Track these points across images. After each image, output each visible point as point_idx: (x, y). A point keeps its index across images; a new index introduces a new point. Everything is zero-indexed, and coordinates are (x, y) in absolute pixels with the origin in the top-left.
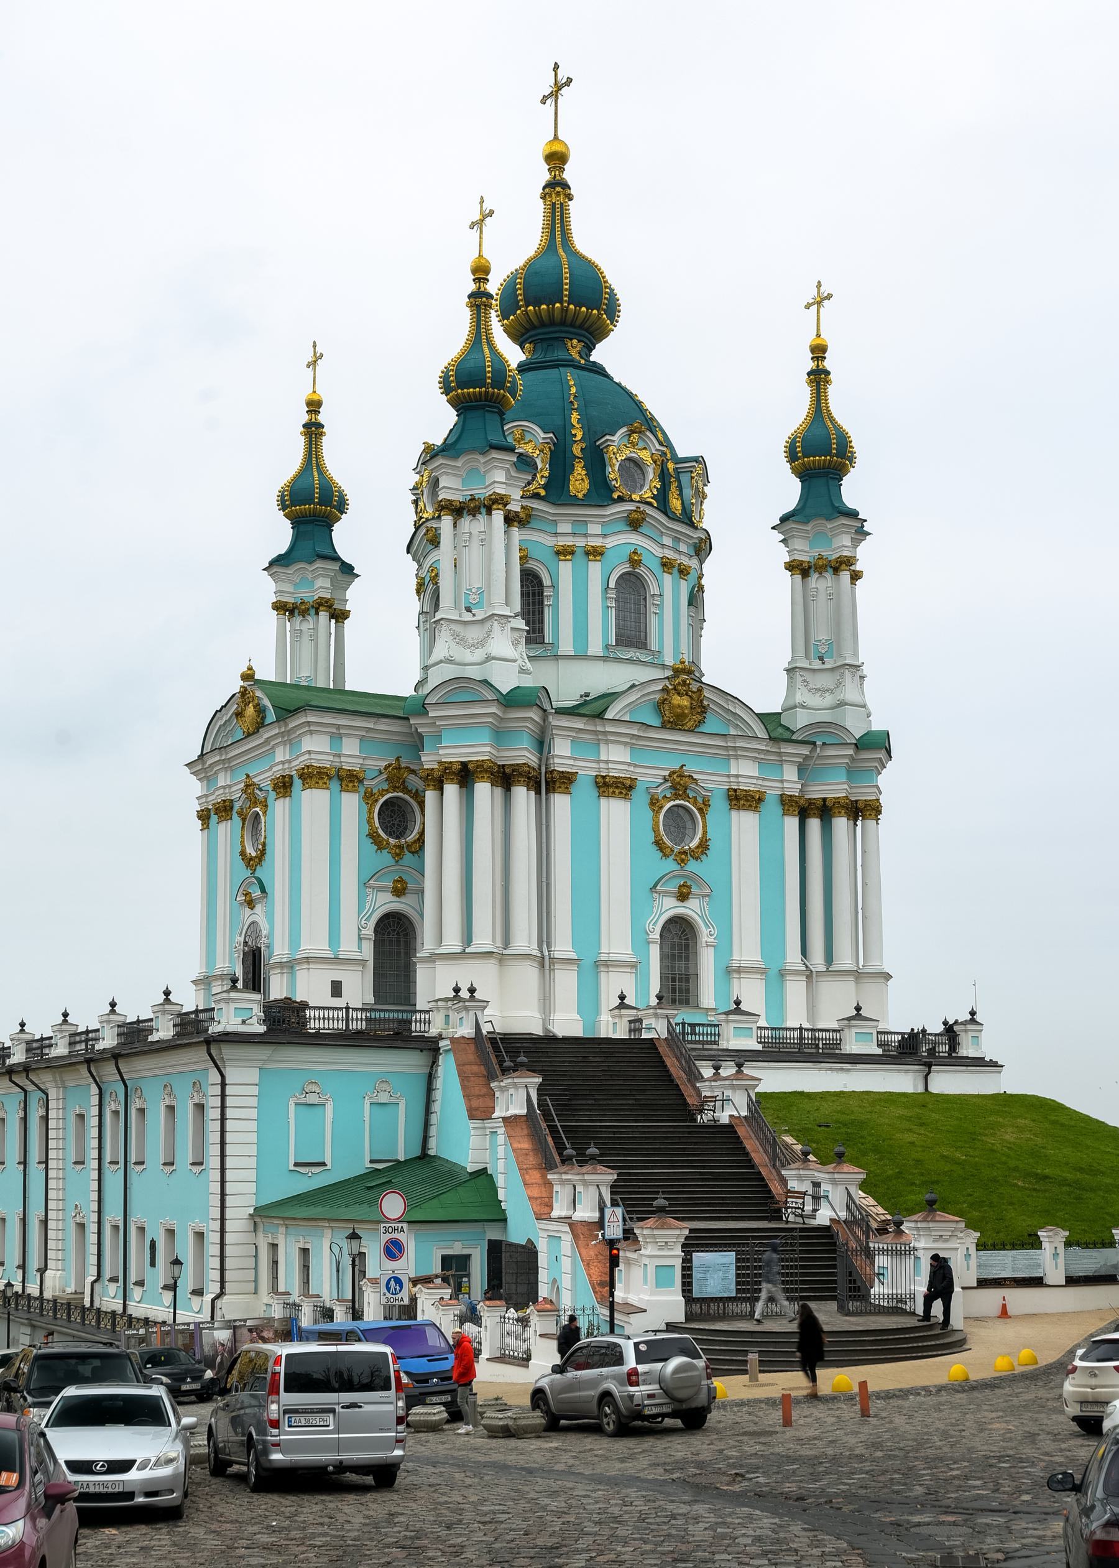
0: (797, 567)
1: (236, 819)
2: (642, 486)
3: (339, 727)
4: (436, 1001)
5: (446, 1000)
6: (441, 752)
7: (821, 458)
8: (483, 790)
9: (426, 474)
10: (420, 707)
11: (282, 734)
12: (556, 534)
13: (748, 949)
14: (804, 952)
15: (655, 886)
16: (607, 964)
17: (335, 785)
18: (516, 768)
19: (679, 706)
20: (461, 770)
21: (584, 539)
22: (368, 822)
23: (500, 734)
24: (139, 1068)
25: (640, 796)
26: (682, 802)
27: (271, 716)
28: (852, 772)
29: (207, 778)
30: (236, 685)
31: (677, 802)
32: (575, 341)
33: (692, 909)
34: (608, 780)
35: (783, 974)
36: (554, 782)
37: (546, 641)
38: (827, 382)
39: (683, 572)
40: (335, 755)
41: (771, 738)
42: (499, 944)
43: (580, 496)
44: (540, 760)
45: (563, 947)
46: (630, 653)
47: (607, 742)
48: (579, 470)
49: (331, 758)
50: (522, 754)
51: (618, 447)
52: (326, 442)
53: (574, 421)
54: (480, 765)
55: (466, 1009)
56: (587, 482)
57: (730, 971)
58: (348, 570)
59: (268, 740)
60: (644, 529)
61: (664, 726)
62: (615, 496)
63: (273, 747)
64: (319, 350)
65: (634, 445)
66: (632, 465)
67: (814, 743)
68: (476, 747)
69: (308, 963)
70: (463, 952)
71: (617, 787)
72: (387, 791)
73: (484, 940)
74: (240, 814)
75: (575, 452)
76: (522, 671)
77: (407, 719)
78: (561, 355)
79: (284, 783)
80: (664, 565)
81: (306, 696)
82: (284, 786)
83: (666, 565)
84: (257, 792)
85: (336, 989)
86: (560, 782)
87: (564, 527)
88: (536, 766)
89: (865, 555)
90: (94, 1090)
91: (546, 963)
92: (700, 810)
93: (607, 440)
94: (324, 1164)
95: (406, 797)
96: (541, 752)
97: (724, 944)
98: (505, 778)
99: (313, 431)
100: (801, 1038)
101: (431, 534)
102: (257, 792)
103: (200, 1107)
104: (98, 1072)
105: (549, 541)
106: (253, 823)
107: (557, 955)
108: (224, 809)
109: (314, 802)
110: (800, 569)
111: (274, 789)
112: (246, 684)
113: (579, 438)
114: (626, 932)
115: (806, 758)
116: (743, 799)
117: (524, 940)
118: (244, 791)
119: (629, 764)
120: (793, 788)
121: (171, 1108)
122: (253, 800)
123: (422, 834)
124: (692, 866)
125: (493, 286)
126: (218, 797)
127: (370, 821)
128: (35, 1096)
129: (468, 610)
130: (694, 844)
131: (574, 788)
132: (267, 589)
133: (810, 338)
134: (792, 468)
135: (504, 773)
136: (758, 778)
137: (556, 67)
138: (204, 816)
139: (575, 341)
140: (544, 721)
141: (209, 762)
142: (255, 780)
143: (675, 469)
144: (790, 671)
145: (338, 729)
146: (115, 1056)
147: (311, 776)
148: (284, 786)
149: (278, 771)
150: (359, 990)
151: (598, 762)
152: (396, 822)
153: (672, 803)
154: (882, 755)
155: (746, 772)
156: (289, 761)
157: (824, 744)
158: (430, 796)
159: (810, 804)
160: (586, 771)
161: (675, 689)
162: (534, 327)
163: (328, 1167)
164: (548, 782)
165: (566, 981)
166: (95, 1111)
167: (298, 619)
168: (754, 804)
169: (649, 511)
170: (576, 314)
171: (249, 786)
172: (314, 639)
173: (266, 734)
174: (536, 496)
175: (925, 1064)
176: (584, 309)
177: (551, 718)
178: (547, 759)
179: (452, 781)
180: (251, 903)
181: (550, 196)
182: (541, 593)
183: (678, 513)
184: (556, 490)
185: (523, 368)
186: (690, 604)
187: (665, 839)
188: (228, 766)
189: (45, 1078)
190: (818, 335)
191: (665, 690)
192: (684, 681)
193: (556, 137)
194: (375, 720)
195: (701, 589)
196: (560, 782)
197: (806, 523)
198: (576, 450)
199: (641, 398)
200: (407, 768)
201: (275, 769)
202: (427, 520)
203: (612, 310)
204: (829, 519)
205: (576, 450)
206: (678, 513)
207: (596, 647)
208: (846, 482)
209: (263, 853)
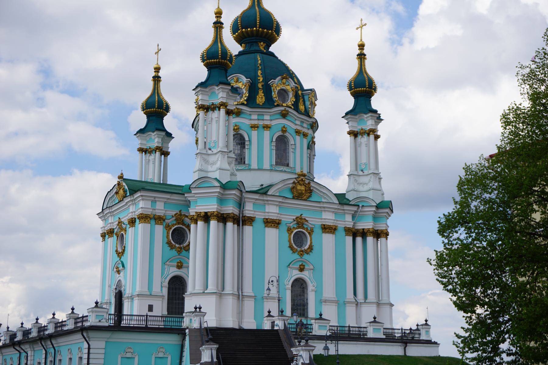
1: (115, 237)
2: (288, 100)
3: (155, 197)
6: (197, 208)
7: (363, 89)
8: (213, 223)
10: (189, 189)
12: (251, 119)
13: (329, 292)
14: (355, 294)
15: (289, 265)
17: (153, 222)
18: (228, 214)
19: (300, 190)
21: (262, 121)
22: (167, 237)
23: (221, 200)
24: (61, 342)
26: (301, 230)
27: (128, 194)
28: (375, 218)
29: (105, 220)
31: (299, 230)
33: (305, 275)
35: (345, 303)
36: (245, 221)
37: (246, 163)
38: (365, 59)
39: (305, 135)
40: (153, 209)
41: (340, 204)
42: (220, 288)
43: (261, 104)
44: (240, 211)
47: (269, 204)
48: (261, 93)
49: (151, 210)
50: (230, 208)
51: (277, 84)
53: (259, 74)
55: (196, 316)
56: (264, 98)
57: (321, 301)
60: (288, 118)
61: (294, 198)
62: (276, 104)
64: (160, 47)
65: (284, 84)
66: (283, 92)
67: (358, 206)
68: (211, 206)
70: (204, 293)
72: (176, 225)
73: (211, 288)
74: (116, 234)
76: (232, 174)
77: (184, 194)
78: (257, 48)
80: (296, 132)
81: (144, 185)
82: (132, 222)
83: (298, 132)
85: (151, 308)
86: (249, 221)
88: (238, 214)
89: (381, 129)
90: (44, 352)
91: (240, 296)
92: (309, 233)
95: (184, 227)
96: (240, 208)
97: (318, 291)
98: (223, 218)
100: (349, 331)
103: (81, 358)
105: (248, 122)
107: (245, 294)
108: (111, 232)
110: (354, 134)
113: (261, 81)
115: (356, 212)
116: (328, 229)
118: (118, 225)
120: (350, 225)
121: (71, 359)
122: (121, 229)
123: (189, 243)
124: (306, 256)
125: (228, 21)
126: (108, 228)
128: (24, 354)
130: (306, 247)
131: (254, 224)
134: (351, 93)
135: (223, 217)
136: (334, 220)
138: (103, 236)
139: (262, 43)
141: (105, 213)
142: (122, 220)
143: (302, 94)
146: (51, 337)
147: (142, 218)
148: (132, 222)
149: (130, 216)
150: (161, 308)
151: (265, 212)
152: (178, 237)
153: (297, 230)
154: (387, 210)
155: (329, 218)
156: (135, 212)
158: (192, 226)
160: (259, 216)
161: (298, 182)
162: (246, 38)
164: (242, 221)
165: (249, 305)
166: (43, 361)
167: (148, 155)
168: (333, 231)
169: (290, 110)
170: (263, 32)
174: (243, 104)
175: (404, 343)
177: (244, 194)
178: (243, 211)
180: (119, 272)
182: (244, 143)
183: (303, 111)
184: (251, 102)
185: (241, 54)
186: (308, 148)
187: (294, 245)
189: (26, 347)
190: (361, 40)
191: (294, 183)
192: (302, 179)
195: (314, 143)
196: (249, 221)
197: (356, 115)
198: (260, 86)
200: (184, 215)
203: (278, 30)
205: (260, 86)
206: (303, 111)
207: (267, 166)
208: (373, 99)
209: (124, 250)
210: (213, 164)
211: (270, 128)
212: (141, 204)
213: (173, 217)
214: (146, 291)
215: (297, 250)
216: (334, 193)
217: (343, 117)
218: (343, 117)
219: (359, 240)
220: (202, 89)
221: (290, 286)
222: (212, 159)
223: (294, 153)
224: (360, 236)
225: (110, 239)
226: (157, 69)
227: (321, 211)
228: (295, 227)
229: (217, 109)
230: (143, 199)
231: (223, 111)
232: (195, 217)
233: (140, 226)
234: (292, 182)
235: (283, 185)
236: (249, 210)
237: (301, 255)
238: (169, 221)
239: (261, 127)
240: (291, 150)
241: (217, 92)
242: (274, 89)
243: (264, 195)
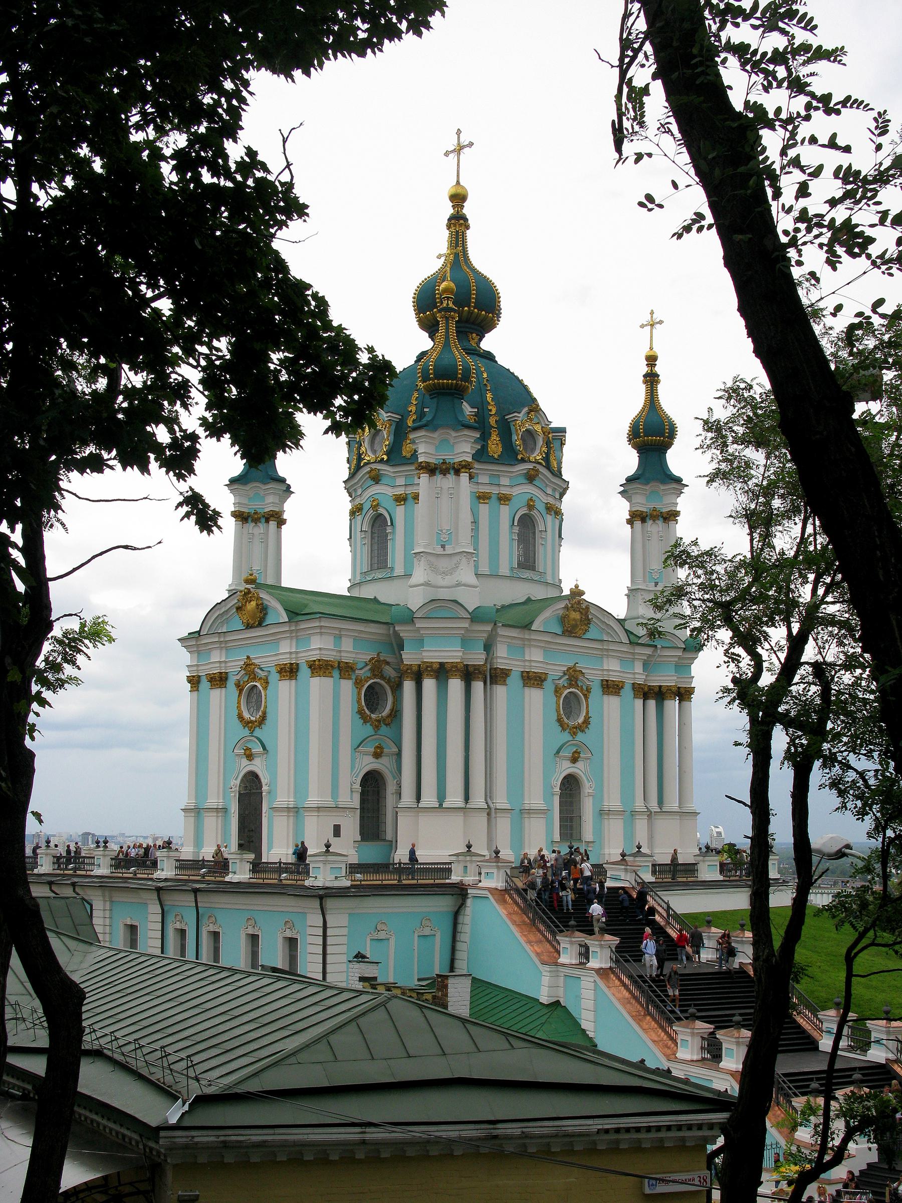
3: (341, 629)
8: (456, 685)
11: (291, 631)
16: (530, 811)
17: (336, 673)
19: (574, 619)
20: (440, 668)
23: (465, 642)
25: (549, 685)
29: (199, 652)
32: (474, 335)
33: (579, 769)
35: (633, 813)
36: (496, 676)
38: (658, 382)
43: (496, 456)
44: (486, 659)
45: (501, 801)
46: (527, 574)
47: (530, 646)
48: (495, 437)
53: (489, 400)
54: (454, 666)
56: (500, 446)
57: (603, 813)
62: (519, 457)
65: (531, 420)
69: (318, 811)
74: (238, 685)
84: (259, 671)
86: (497, 676)
91: (490, 812)
95: (382, 682)
98: (468, 674)
101: (373, 473)
109: (318, 687)
110: (635, 517)
113: (493, 412)
116: (611, 688)
120: (640, 679)
122: (253, 676)
124: (580, 736)
127: (359, 701)
130: (581, 720)
131: (509, 680)
133: (645, 351)
137: (459, 132)
138: (194, 682)
139: (474, 335)
147: (320, 667)
148: (290, 671)
149: (285, 660)
155: (613, 668)
158: (408, 686)
159: (650, 689)
161: (572, 607)
164: (497, 676)
165: (503, 825)
169: (542, 470)
170: (478, 315)
179: (431, 677)
181: (455, 225)
188: (224, 646)
190: (651, 349)
191: (566, 608)
193: (458, 182)
198: (492, 421)
204: (663, 482)
205: (492, 421)
207: (504, 570)
209: (264, 718)
213: (367, 665)
214: (328, 801)
219: (652, 703)
221: (557, 789)
224: (653, 698)
227: (602, 657)
229: (452, 472)
230: (321, 634)
236: (503, 656)
237: (575, 734)
238: (362, 672)
240: (539, 541)
241: (452, 441)
243: (527, 632)
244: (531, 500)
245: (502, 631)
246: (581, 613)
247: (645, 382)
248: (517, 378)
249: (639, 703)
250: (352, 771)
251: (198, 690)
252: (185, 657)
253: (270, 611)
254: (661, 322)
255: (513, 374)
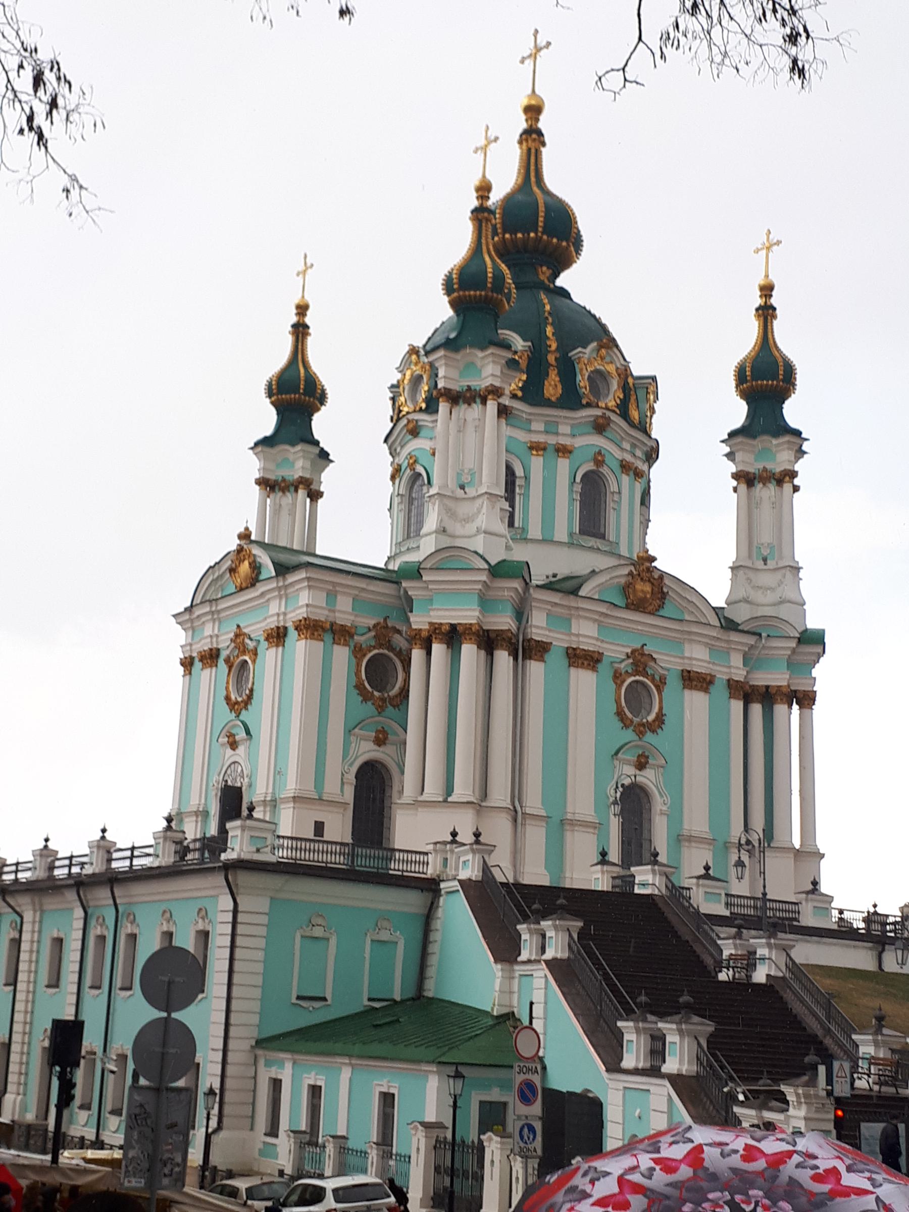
0: (740, 477)
2: (607, 395)
3: (334, 584)
4: (436, 843)
5: (445, 843)
6: (432, 613)
7: (766, 381)
8: (469, 651)
9: (408, 373)
12: (530, 431)
17: (328, 637)
18: (500, 633)
19: (642, 591)
20: (449, 632)
22: (356, 674)
26: (641, 678)
29: (193, 629)
30: (233, 544)
32: (544, 269)
34: (578, 652)
36: (531, 650)
37: (516, 525)
38: (774, 317)
40: (330, 610)
43: (553, 399)
44: (518, 629)
46: (592, 542)
48: (553, 377)
49: (326, 612)
52: (311, 343)
56: (560, 387)
58: (324, 456)
59: (263, 594)
61: (627, 607)
62: (584, 402)
63: (268, 600)
65: (602, 358)
68: (466, 614)
70: (445, 801)
71: (587, 659)
72: (374, 648)
74: (227, 661)
75: (550, 361)
79: (278, 634)
83: (625, 467)
84: (247, 641)
85: (319, 827)
87: (537, 424)
91: (517, 816)
93: (580, 352)
94: (325, 999)
95: (391, 655)
98: (489, 642)
99: (300, 331)
101: (411, 426)
102: (247, 641)
104: (85, 896)
106: (240, 671)
111: (267, 639)
112: (243, 542)
113: (554, 346)
114: (587, 793)
116: (693, 680)
117: (500, 795)
119: (597, 639)
122: (244, 650)
124: (649, 737)
126: (204, 645)
129: (462, 487)
131: (547, 657)
132: (253, 466)
138: (187, 664)
139: (544, 269)
140: (524, 593)
142: (246, 631)
144: (732, 568)
145: (334, 587)
147: (307, 627)
148: (278, 636)
149: (272, 623)
153: (633, 678)
157: (769, 636)
158: (417, 655)
160: (559, 641)
161: (639, 575)
163: (329, 1003)
164: (527, 649)
168: (705, 685)
169: (614, 417)
171: (239, 635)
172: (292, 513)
173: (261, 588)
176: (555, 240)
177: (531, 591)
178: (525, 628)
180: (234, 745)
184: (532, 393)
187: (626, 710)
190: (767, 276)
191: (631, 574)
194: (368, 581)
198: (551, 358)
199: (604, 321)
201: (269, 620)
202: (408, 413)
206: (636, 421)
207: (561, 534)
209: (250, 697)
210: (468, 520)
211: (570, 452)
212: (304, 597)
213: (370, 630)
215: (632, 721)
216: (714, 605)
217: (723, 441)
218: (723, 441)
220: (449, 354)
222: (464, 509)
223: (617, 510)
225: (207, 671)
226: (302, 309)
228: (630, 671)
231: (492, 406)
232: (424, 634)
233: (299, 647)
234: (626, 572)
235: (608, 577)
236: (539, 626)
239: (550, 450)
240: (610, 505)
242: (581, 370)
243: (572, 597)
244: (600, 453)
245: (536, 594)
246: (653, 584)
247: (758, 316)
248: (594, 316)
249: (737, 706)
250: (343, 761)
251: (190, 673)
252: (180, 636)
253: (263, 571)
254: (778, 243)
255: (589, 312)
